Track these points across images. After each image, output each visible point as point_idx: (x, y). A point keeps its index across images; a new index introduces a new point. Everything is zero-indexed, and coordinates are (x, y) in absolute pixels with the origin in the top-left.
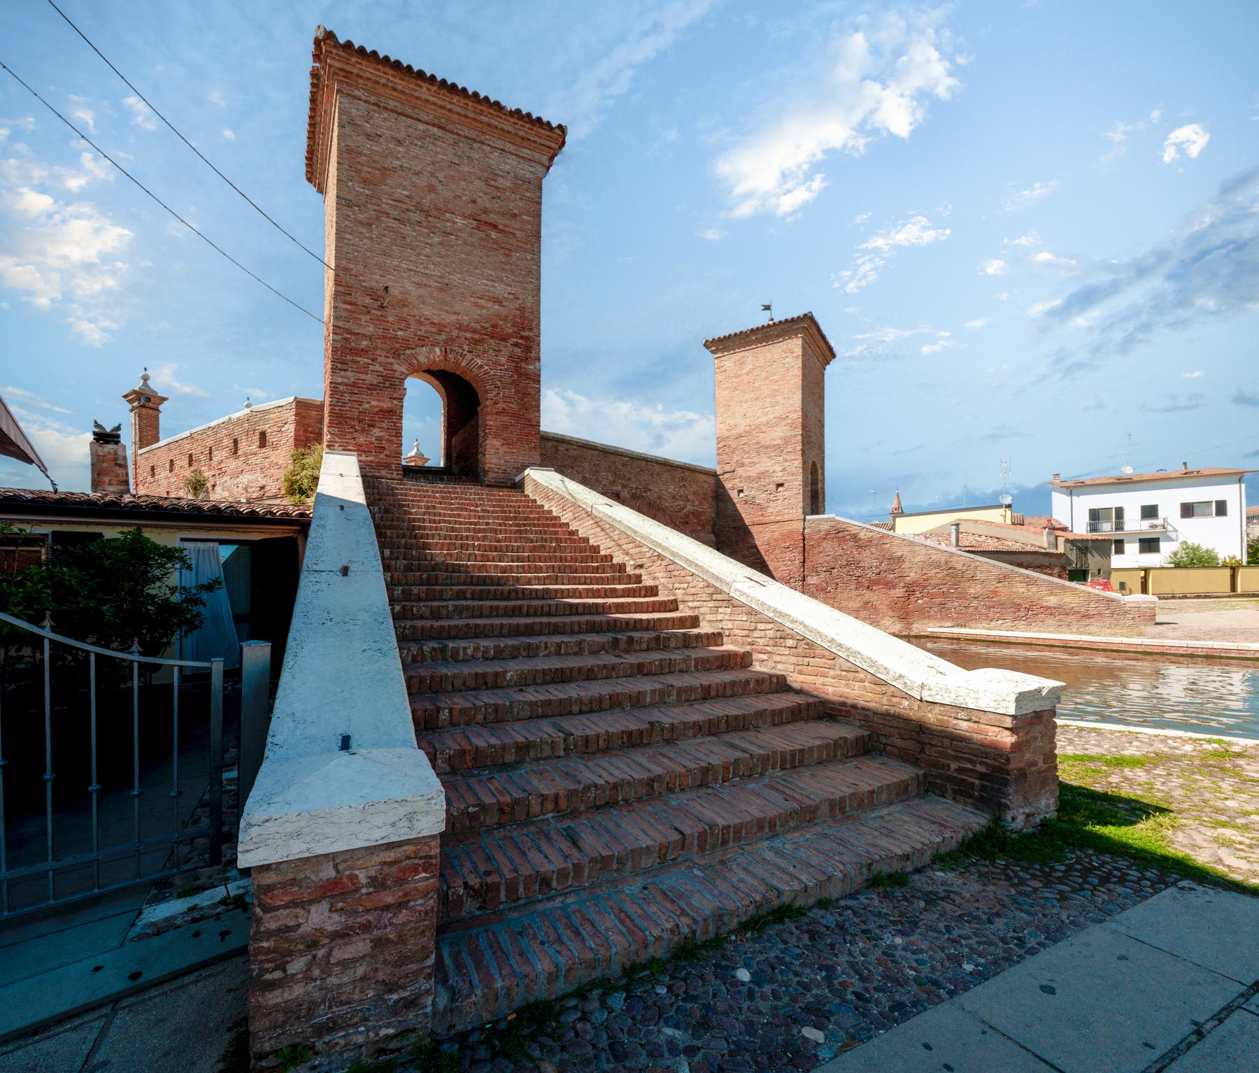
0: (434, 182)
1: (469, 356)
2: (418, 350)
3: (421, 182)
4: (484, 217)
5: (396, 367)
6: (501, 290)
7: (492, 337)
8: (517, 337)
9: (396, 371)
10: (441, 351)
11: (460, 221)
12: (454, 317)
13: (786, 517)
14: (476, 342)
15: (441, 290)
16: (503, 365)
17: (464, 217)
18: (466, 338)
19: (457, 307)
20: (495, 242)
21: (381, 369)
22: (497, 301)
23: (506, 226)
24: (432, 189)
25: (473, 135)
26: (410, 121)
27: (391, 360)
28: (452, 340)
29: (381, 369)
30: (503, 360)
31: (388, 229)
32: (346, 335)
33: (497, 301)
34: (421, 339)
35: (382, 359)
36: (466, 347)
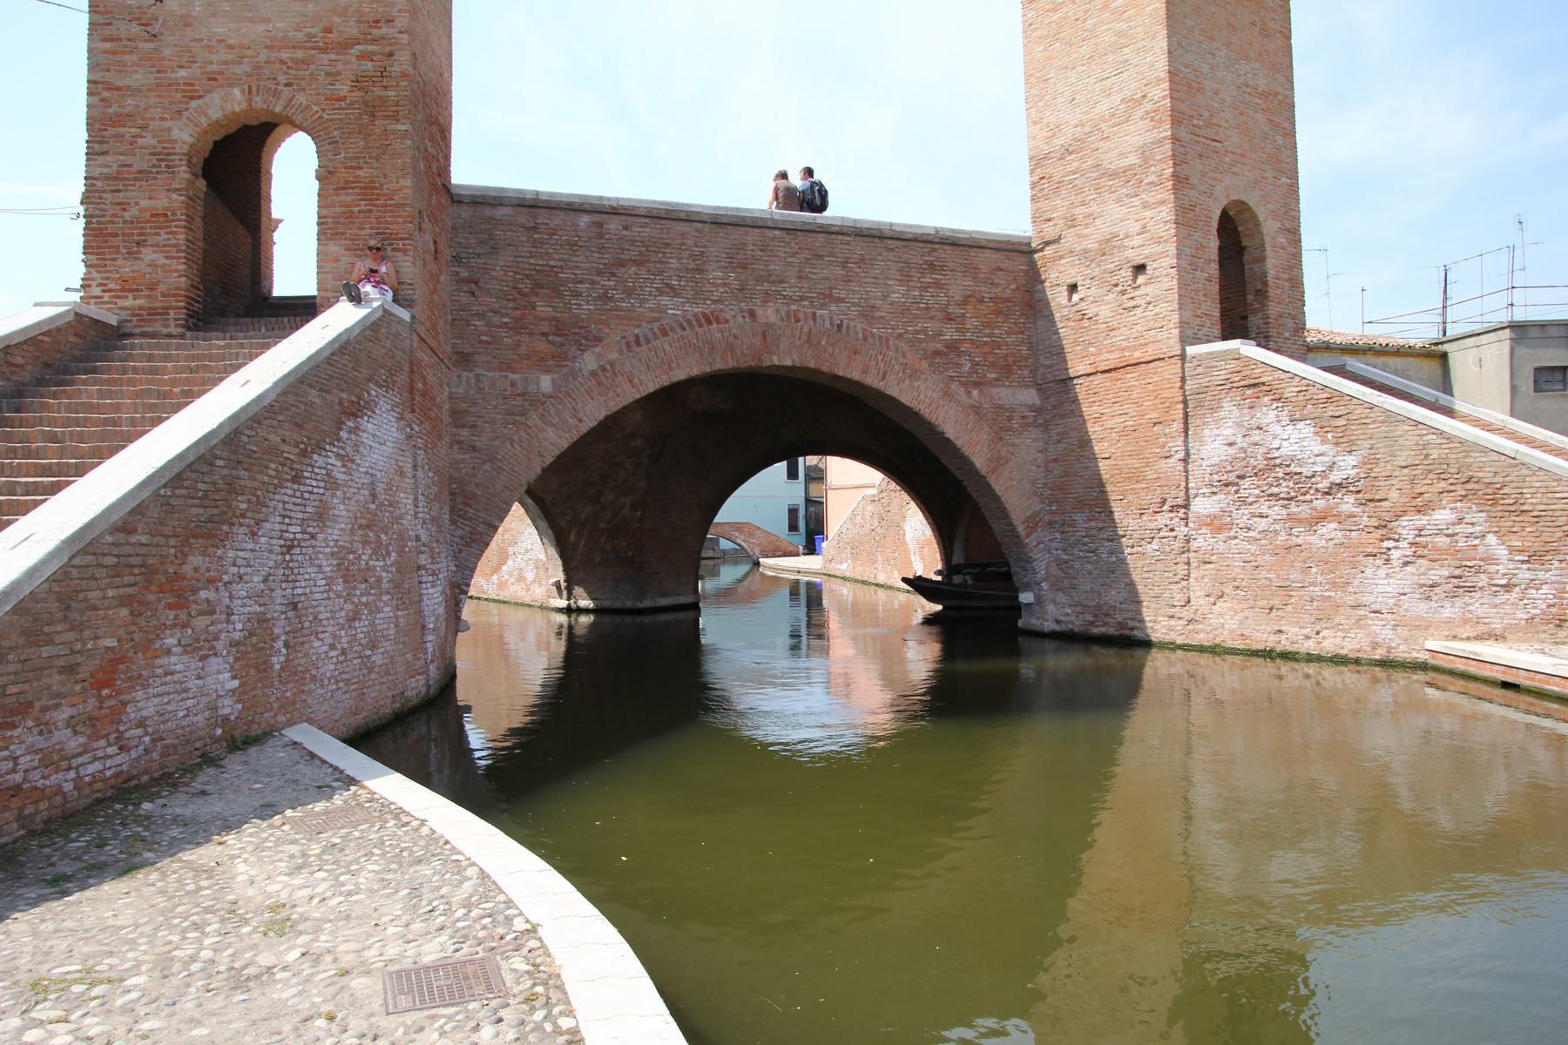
1: (287, 92)
2: (207, 99)
5: (175, 134)
7: (324, 50)
8: (366, 41)
9: (175, 141)
10: (243, 91)
12: (262, 28)
13: (1151, 352)
16: (344, 99)
18: (282, 62)
21: (153, 142)
27: (168, 124)
29: (153, 142)
30: (343, 89)
32: (106, 94)
35: (154, 125)
36: (282, 79)
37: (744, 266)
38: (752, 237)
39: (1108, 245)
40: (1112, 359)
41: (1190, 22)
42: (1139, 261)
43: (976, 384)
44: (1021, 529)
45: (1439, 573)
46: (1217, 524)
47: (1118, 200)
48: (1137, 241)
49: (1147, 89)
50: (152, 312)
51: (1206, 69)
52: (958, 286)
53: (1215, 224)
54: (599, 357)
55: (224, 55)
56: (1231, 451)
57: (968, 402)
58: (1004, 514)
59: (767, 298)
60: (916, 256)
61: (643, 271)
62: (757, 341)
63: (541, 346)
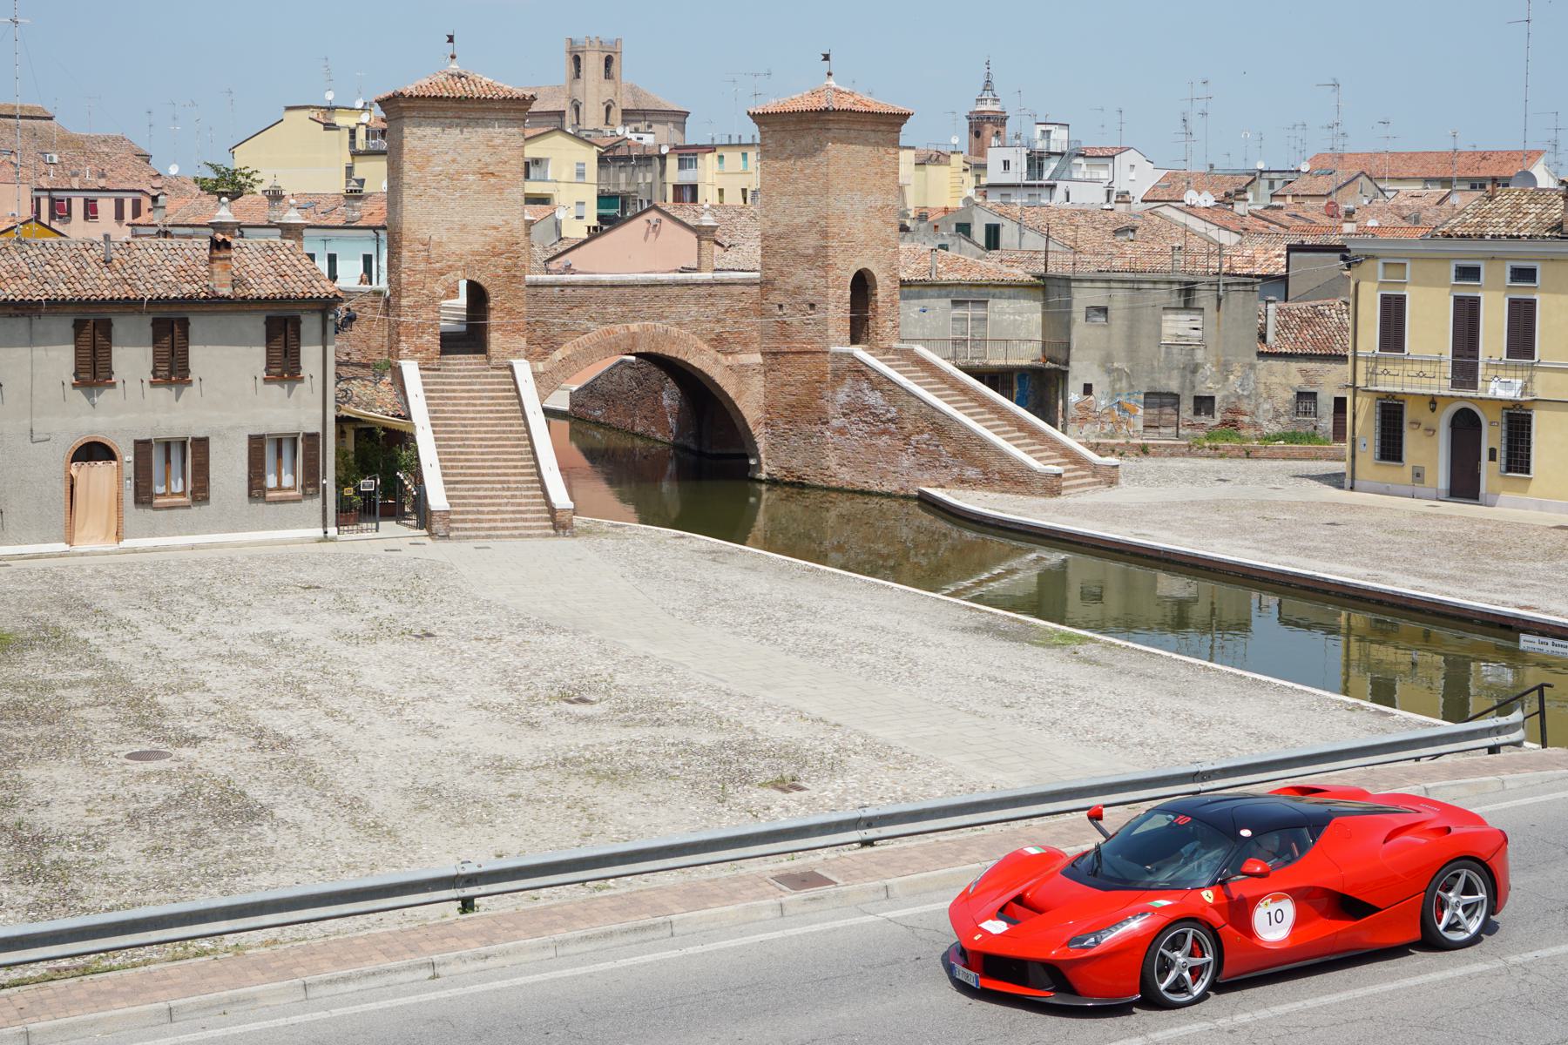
0: (456, 156)
3: (448, 158)
4: (485, 170)
6: (497, 221)
11: (471, 177)
13: (815, 347)
14: (481, 261)
15: (461, 230)
17: (474, 174)
19: (470, 238)
20: (493, 185)
22: (495, 228)
23: (499, 171)
24: (454, 161)
25: (478, 115)
26: (442, 120)
28: (467, 265)
31: (433, 196)
33: (495, 228)
34: (450, 267)
37: (624, 304)
38: (627, 290)
39: (799, 290)
40: (797, 346)
41: (840, 186)
42: (812, 302)
43: (731, 353)
44: (751, 427)
45: (923, 460)
46: (841, 431)
47: (803, 270)
48: (811, 293)
49: (818, 220)
50: (428, 359)
51: (848, 207)
52: (724, 304)
53: (849, 284)
54: (562, 353)
55: (454, 258)
56: (849, 399)
57: (728, 364)
58: (744, 419)
59: (634, 319)
60: (703, 291)
61: (581, 312)
62: (630, 342)
63: (539, 349)
